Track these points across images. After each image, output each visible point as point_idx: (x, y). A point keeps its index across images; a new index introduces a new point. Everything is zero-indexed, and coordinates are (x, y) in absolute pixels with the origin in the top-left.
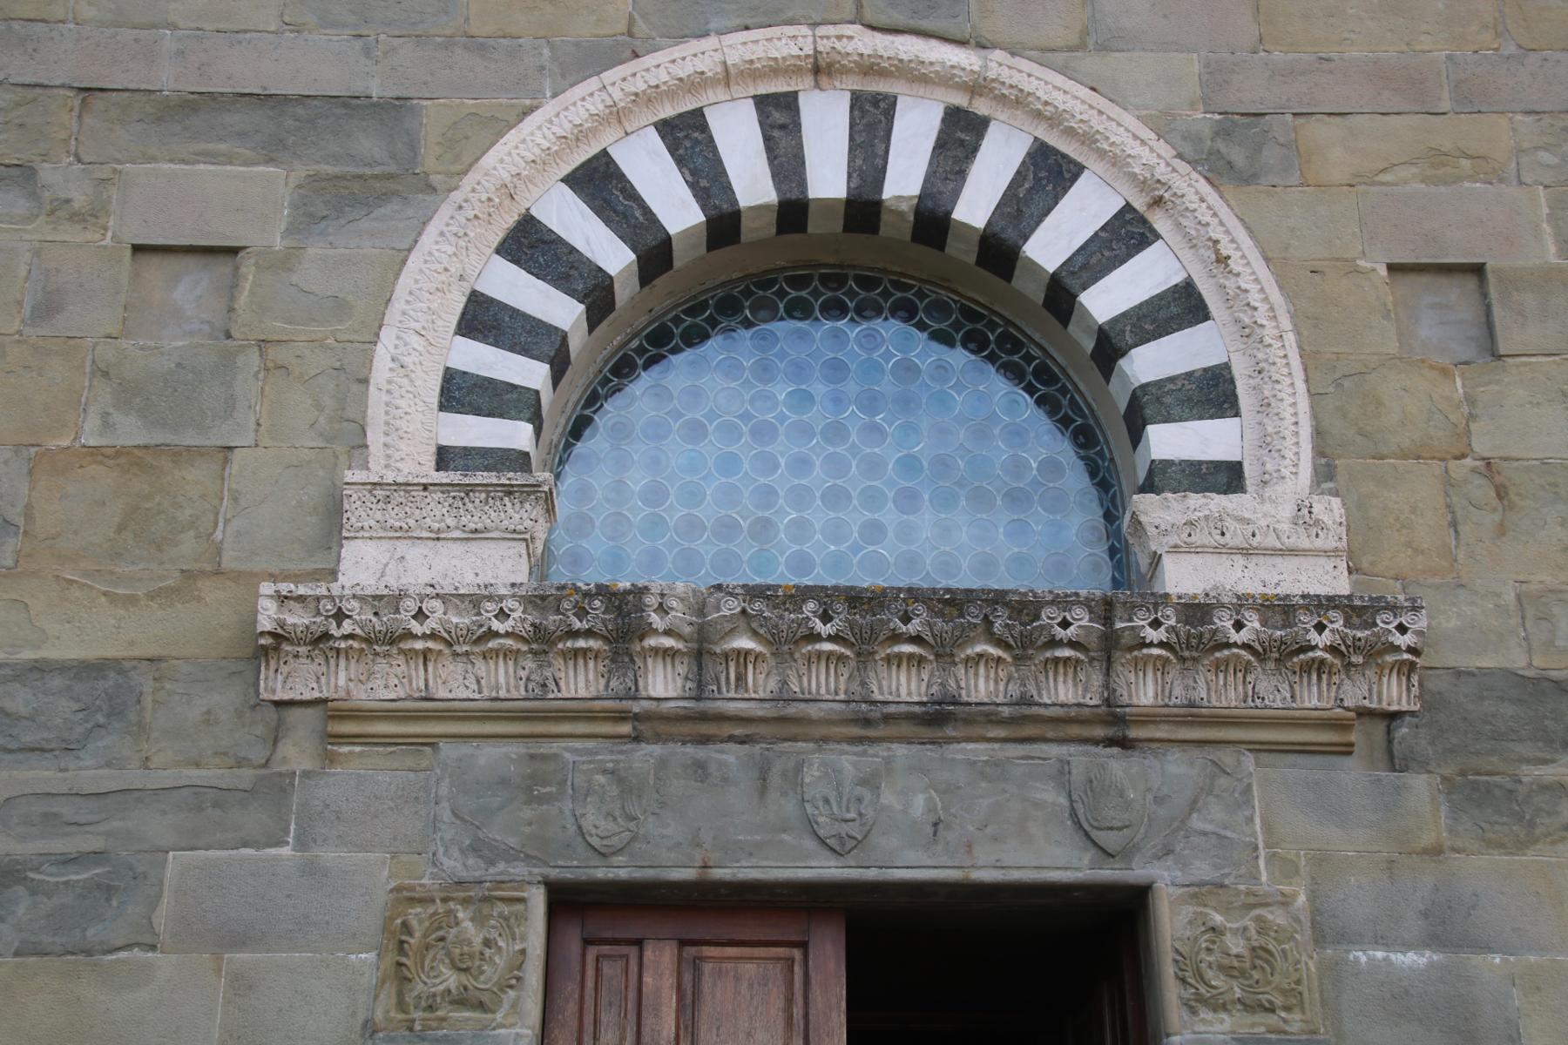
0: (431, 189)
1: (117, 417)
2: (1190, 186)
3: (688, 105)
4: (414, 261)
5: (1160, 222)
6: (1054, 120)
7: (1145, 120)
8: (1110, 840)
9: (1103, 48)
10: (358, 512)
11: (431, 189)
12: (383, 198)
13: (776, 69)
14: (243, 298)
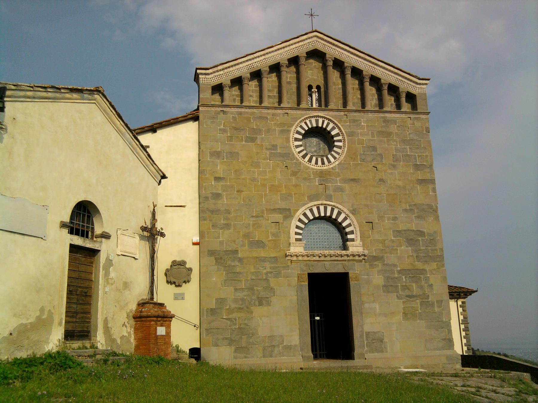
2: (351, 215)
4: (292, 223)
5: (348, 218)
6: (340, 209)
7: (347, 209)
9: (344, 203)
10: (291, 244)
12: (289, 217)
13: (318, 205)
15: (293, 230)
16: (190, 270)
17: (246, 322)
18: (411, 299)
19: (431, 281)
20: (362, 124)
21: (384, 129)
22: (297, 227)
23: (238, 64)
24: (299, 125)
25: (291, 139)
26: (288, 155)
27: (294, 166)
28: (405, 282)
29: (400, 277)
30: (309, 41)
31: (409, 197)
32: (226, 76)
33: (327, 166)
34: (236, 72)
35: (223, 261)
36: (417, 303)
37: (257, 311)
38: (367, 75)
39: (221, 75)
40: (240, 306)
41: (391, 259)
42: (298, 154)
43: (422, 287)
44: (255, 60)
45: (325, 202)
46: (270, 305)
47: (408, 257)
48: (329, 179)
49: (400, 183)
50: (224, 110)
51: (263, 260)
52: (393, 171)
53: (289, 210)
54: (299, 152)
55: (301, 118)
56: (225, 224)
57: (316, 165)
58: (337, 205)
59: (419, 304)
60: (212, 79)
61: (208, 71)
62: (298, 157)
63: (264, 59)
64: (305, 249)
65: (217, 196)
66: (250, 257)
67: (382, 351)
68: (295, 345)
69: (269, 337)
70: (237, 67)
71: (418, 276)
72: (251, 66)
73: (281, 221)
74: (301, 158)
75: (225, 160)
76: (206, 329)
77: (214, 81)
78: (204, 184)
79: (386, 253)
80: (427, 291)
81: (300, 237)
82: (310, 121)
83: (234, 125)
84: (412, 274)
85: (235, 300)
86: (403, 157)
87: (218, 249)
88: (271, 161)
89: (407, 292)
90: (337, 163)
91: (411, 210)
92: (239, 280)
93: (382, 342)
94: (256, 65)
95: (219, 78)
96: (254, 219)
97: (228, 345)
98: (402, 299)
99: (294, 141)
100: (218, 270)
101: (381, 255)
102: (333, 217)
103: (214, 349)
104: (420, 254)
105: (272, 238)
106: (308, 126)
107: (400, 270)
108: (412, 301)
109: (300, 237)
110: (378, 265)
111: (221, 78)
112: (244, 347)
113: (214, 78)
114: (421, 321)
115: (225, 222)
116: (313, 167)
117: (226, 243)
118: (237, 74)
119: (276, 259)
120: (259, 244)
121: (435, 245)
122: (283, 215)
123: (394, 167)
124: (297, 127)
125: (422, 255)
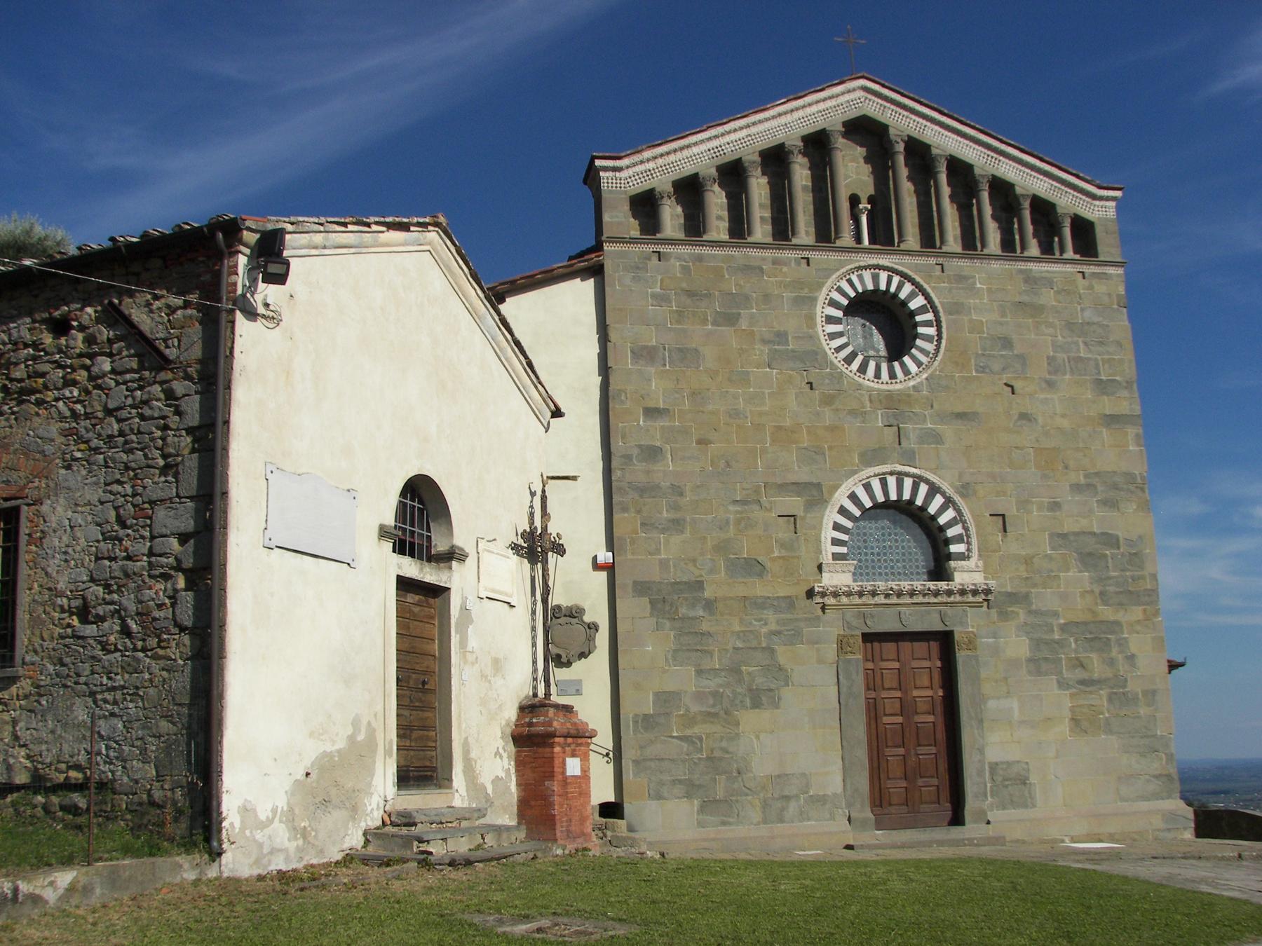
0: (826, 501)
3: (868, 480)
7: (950, 485)
8: (947, 624)
10: (825, 568)
11: (826, 501)
13: (884, 474)
14: (798, 526)
15: (829, 533)
16: (593, 627)
17: (724, 744)
18: (1088, 689)
19: (1133, 648)
20: (978, 286)
21: (1025, 298)
22: (837, 527)
23: (688, 146)
24: (835, 287)
25: (819, 320)
26: (814, 357)
27: (827, 381)
28: (1076, 651)
29: (1065, 639)
30: (847, 97)
31: (1085, 456)
32: (662, 173)
33: (901, 382)
34: (684, 165)
35: (667, 608)
36: (1100, 698)
37: (749, 719)
38: (983, 176)
39: (650, 171)
40: (708, 710)
41: (1046, 599)
42: (835, 355)
43: (1112, 662)
44: (728, 138)
45: (899, 468)
46: (777, 707)
47: (1083, 594)
48: (907, 414)
49: (1065, 424)
50: (662, 250)
51: (761, 604)
52: (1048, 396)
53: (818, 486)
54: (838, 349)
55: (838, 270)
56: (673, 520)
57: (876, 380)
58: (925, 475)
59: (1105, 699)
60: (629, 180)
61: (620, 161)
62: (836, 361)
63: (747, 136)
64: (856, 576)
65: (652, 453)
66: (731, 598)
67: (1025, 806)
68: (835, 795)
69: (775, 776)
70: (686, 153)
71: (1103, 636)
72: (719, 151)
73: (799, 512)
74: (842, 362)
75: (668, 367)
76: (633, 761)
77: (634, 185)
78: (620, 425)
79: (1035, 585)
80: (1122, 667)
81: (844, 550)
82: (861, 278)
83: (684, 285)
84: (1091, 633)
85: (699, 696)
86: (1069, 362)
87: (657, 579)
88: (775, 371)
89: (1080, 674)
90: (925, 376)
91: (1089, 486)
92: (706, 651)
93: (1025, 784)
94: (729, 150)
95: (647, 178)
96: (739, 509)
97: (684, 797)
98: (1068, 687)
99: (824, 324)
100: (659, 627)
101: (1024, 590)
102: (916, 503)
103: (653, 805)
104: (1107, 588)
106: (855, 289)
107: (1065, 624)
108: (1091, 693)
109: (844, 550)
110: (1017, 614)
111: (650, 177)
112: (719, 801)
113: (633, 179)
114: (1110, 737)
115: (672, 515)
116: (872, 384)
117: (674, 566)
118: (688, 170)
119: (790, 602)
120: (754, 567)
121: (1142, 568)
122: (804, 499)
123: (1050, 385)
124: (830, 291)
125: (1112, 589)
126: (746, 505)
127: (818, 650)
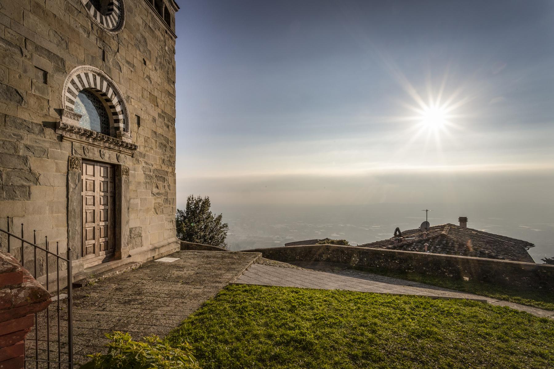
1: (36, 91)
13: (96, 72)
18: (159, 197)
48: (108, 47)
59: (162, 201)
73: (50, 71)
79: (147, 151)
93: (140, 236)
105: (35, 92)
126: (9, 45)
127: (57, 164)
